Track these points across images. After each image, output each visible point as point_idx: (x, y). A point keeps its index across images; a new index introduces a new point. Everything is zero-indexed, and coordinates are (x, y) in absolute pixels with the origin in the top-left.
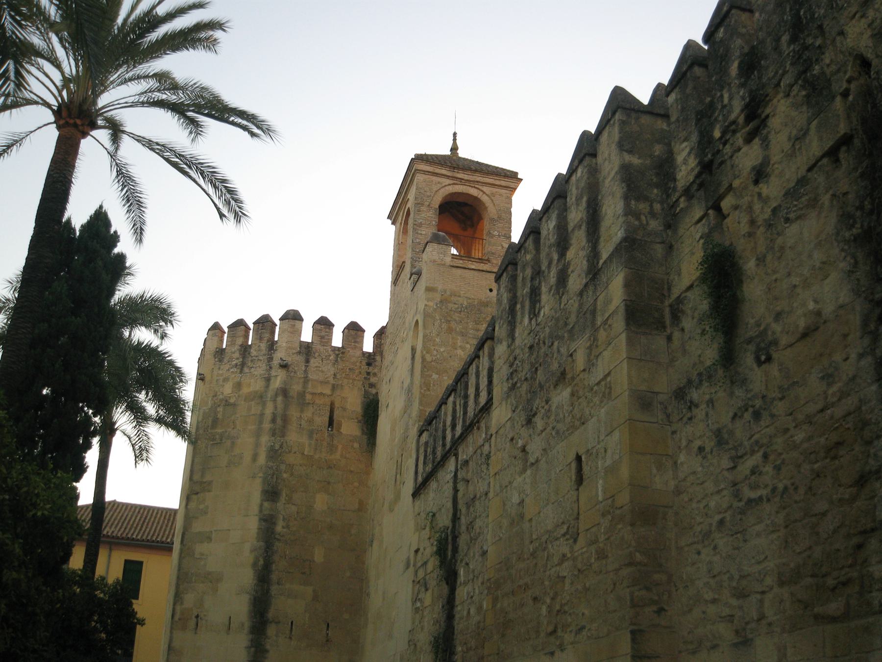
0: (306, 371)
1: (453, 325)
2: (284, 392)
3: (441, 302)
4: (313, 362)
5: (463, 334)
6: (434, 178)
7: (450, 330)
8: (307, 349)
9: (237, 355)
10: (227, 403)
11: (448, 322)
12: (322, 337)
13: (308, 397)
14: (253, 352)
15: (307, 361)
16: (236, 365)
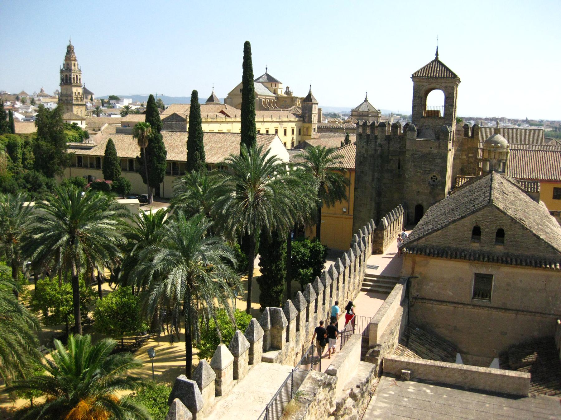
0: (389, 147)
1: (416, 163)
2: (381, 156)
3: (412, 155)
4: (392, 143)
5: (419, 167)
6: (421, 84)
7: (415, 166)
8: (388, 138)
9: (365, 137)
10: (364, 157)
11: (414, 162)
12: (394, 133)
13: (390, 157)
14: (371, 138)
15: (389, 143)
16: (365, 142)
